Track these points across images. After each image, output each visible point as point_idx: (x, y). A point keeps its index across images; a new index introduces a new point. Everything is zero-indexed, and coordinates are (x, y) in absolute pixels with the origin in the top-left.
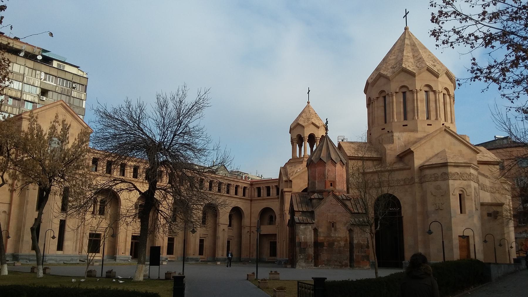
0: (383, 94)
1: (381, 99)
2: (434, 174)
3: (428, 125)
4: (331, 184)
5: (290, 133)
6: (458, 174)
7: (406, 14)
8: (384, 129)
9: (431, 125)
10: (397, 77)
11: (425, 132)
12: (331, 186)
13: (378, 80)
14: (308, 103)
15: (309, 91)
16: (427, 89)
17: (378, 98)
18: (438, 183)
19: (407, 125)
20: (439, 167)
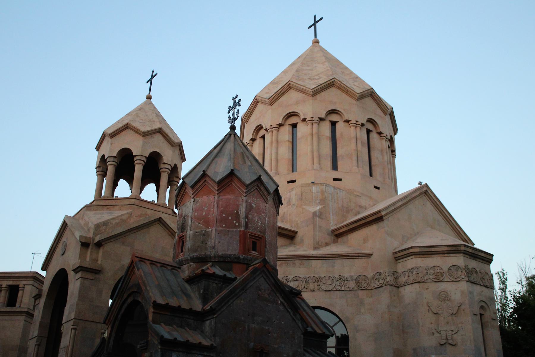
0: (293, 120)
1: (287, 129)
2: (433, 268)
3: (375, 187)
4: (254, 244)
5: (98, 148)
6: (476, 272)
7: (316, 22)
8: (294, 181)
9: (378, 188)
10: (323, 93)
11: (371, 198)
12: (254, 250)
13: (283, 94)
14: (149, 97)
15: (153, 76)
16: (370, 126)
17: (280, 125)
18: (442, 286)
19: (340, 180)
20: (443, 253)
